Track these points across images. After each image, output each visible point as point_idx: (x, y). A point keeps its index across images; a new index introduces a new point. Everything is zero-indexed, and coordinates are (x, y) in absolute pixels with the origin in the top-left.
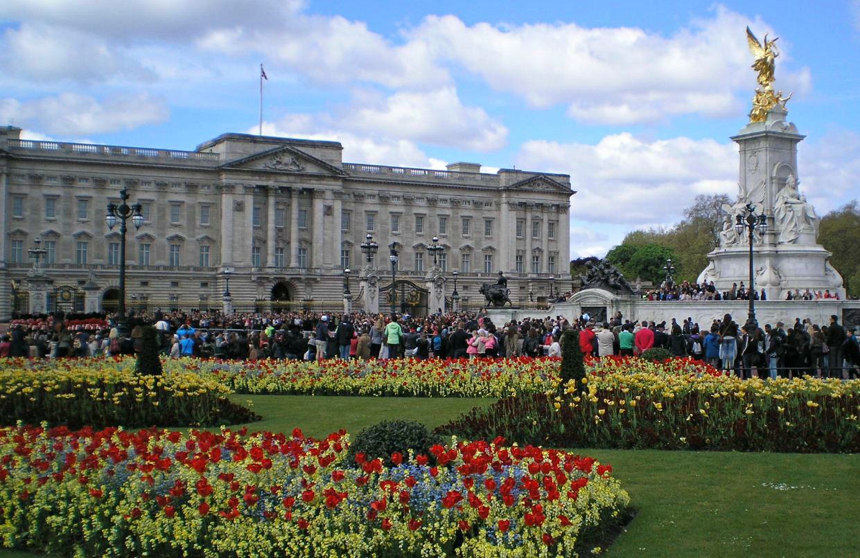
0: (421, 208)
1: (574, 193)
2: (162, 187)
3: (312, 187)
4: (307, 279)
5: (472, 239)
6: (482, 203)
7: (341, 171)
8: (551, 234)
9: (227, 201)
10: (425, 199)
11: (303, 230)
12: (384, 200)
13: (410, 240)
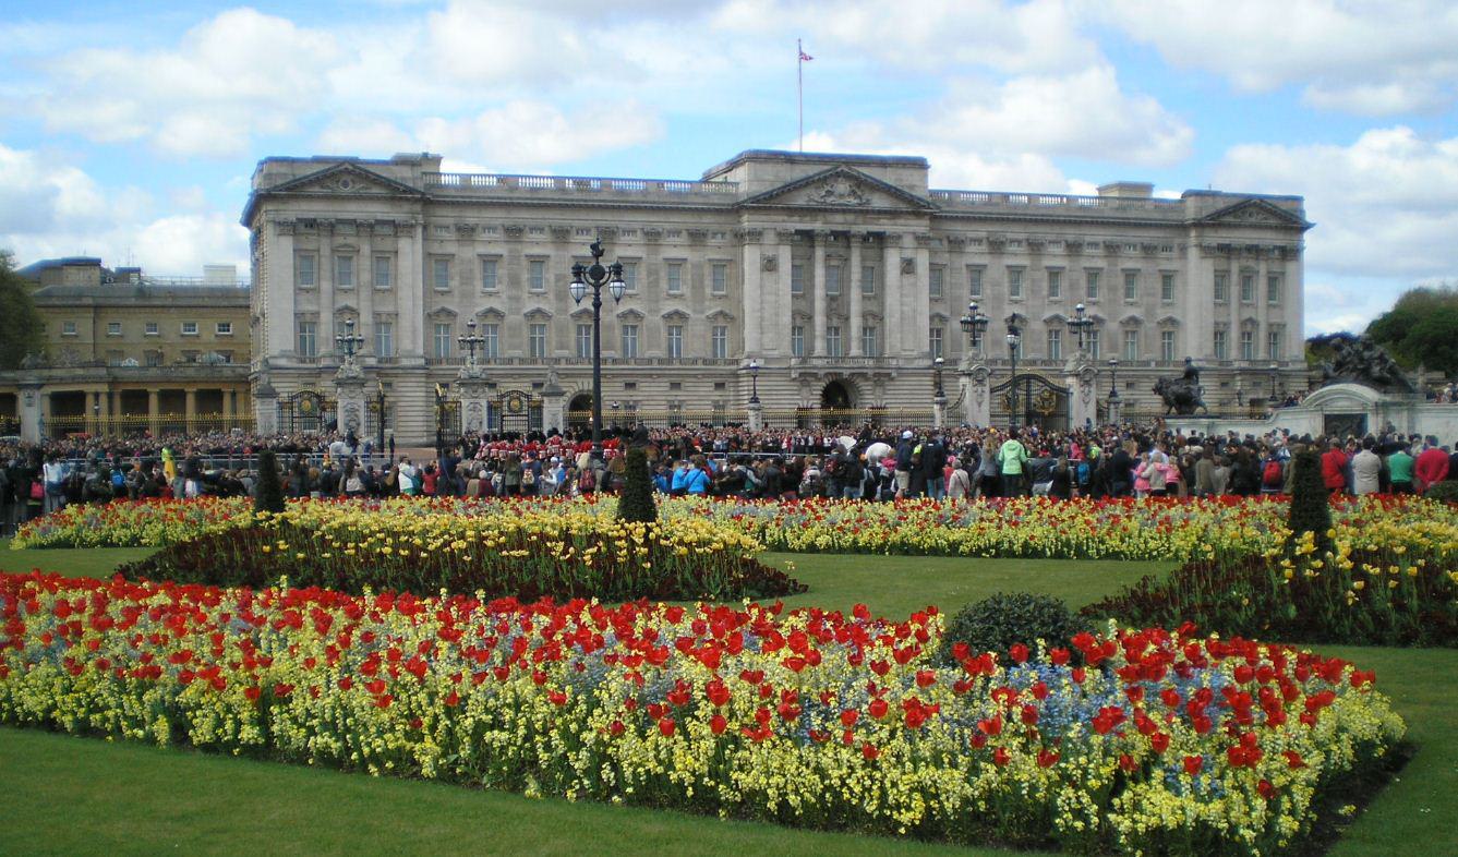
0: (1055, 257)
1: (1308, 226)
2: (653, 237)
4: (875, 375)
6: (1155, 248)
8: (1271, 294)
9: (751, 256)
10: (1063, 244)
11: (869, 298)
12: (997, 247)
13: (1038, 309)
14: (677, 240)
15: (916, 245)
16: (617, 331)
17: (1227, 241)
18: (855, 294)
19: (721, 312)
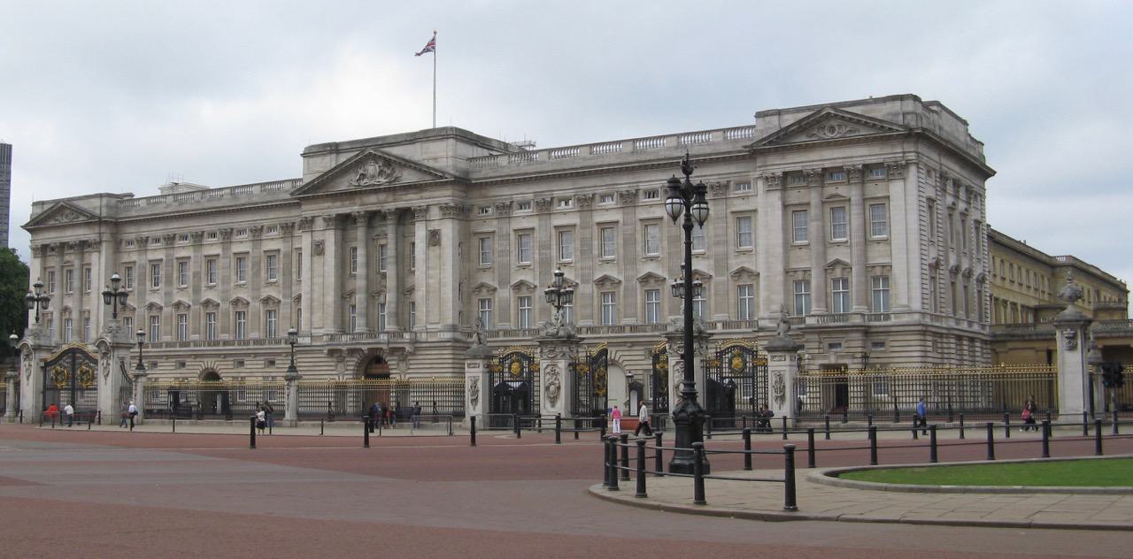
5: (708, 258)
6: (727, 186)
7: (443, 172)
12: (545, 207)
16: (231, 317)
17: (798, 167)
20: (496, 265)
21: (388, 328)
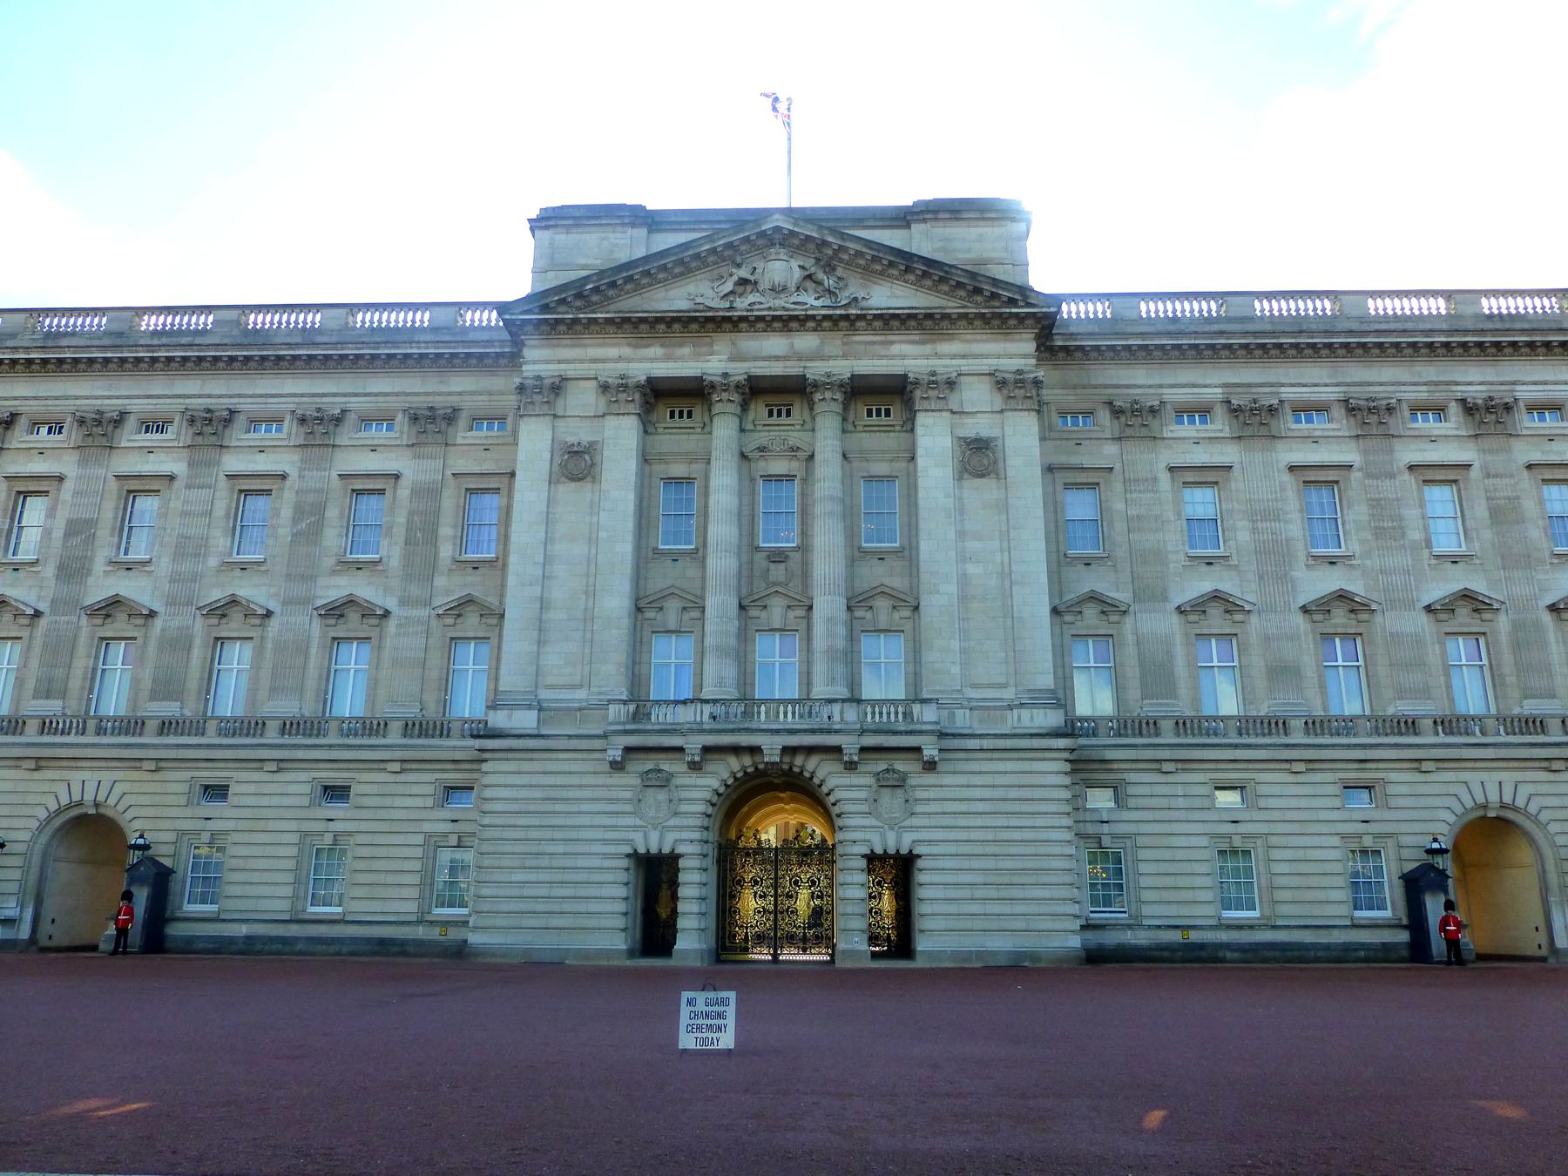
3: (899, 371)
7: (1025, 291)
9: (535, 442)
10: (1454, 409)
12: (1255, 419)
14: (377, 434)
15: (998, 403)
16: (197, 654)
18: (828, 543)
19: (468, 601)
20: (1121, 553)
21: (820, 690)
